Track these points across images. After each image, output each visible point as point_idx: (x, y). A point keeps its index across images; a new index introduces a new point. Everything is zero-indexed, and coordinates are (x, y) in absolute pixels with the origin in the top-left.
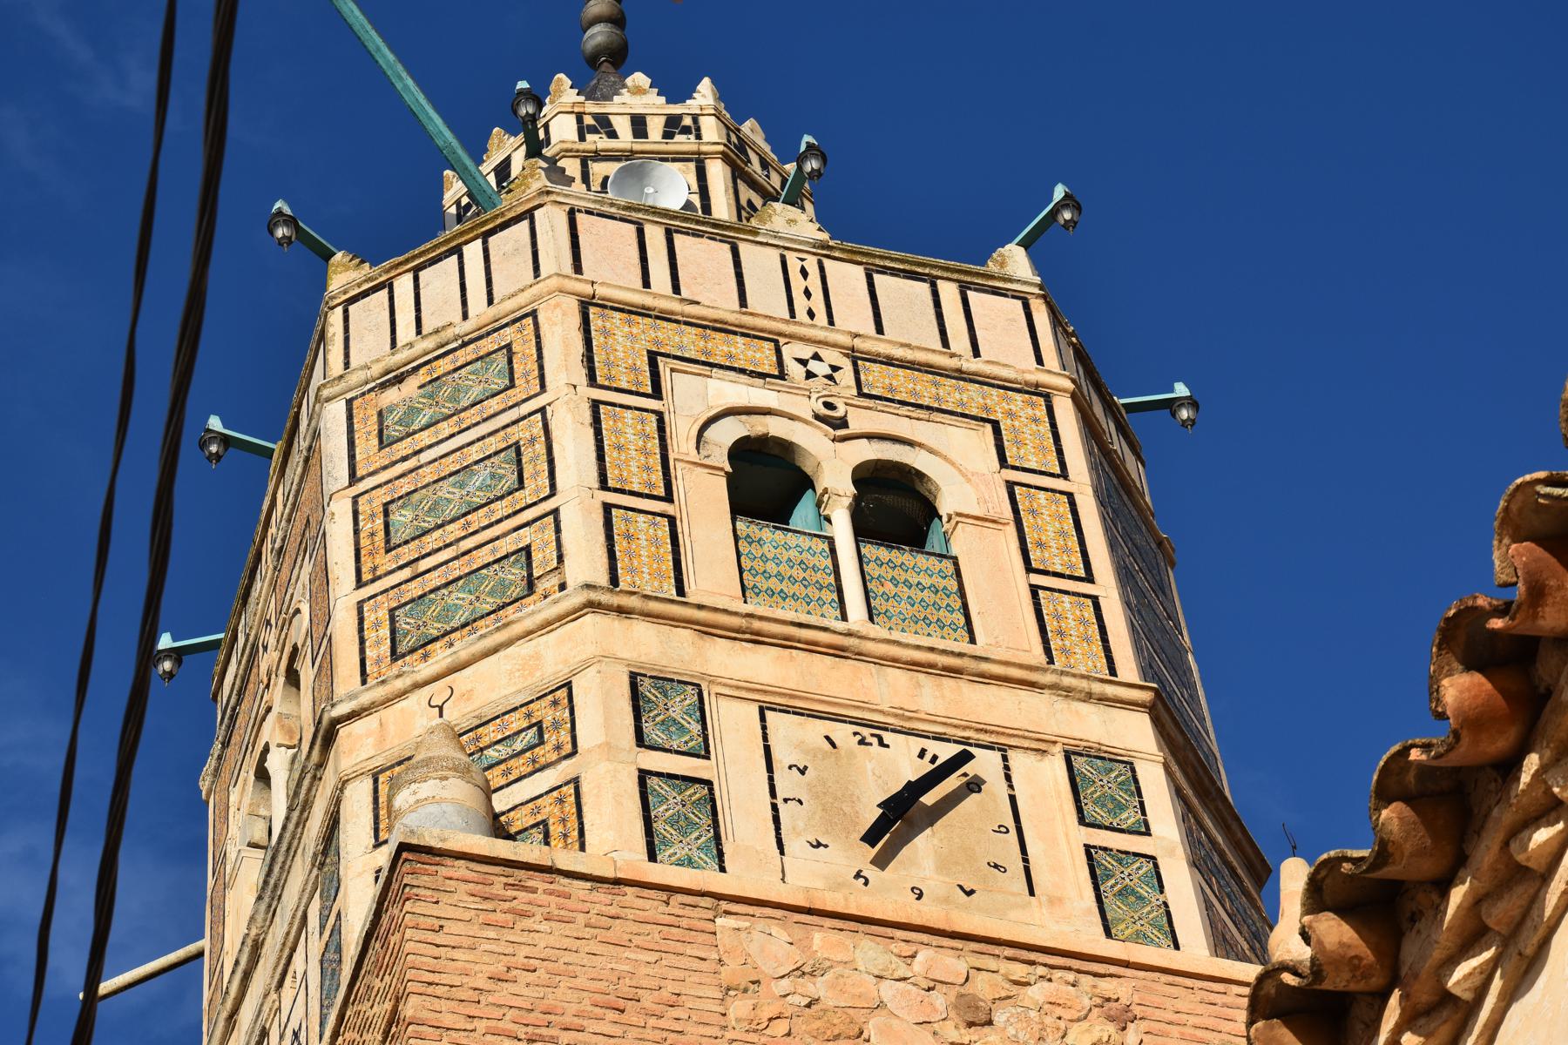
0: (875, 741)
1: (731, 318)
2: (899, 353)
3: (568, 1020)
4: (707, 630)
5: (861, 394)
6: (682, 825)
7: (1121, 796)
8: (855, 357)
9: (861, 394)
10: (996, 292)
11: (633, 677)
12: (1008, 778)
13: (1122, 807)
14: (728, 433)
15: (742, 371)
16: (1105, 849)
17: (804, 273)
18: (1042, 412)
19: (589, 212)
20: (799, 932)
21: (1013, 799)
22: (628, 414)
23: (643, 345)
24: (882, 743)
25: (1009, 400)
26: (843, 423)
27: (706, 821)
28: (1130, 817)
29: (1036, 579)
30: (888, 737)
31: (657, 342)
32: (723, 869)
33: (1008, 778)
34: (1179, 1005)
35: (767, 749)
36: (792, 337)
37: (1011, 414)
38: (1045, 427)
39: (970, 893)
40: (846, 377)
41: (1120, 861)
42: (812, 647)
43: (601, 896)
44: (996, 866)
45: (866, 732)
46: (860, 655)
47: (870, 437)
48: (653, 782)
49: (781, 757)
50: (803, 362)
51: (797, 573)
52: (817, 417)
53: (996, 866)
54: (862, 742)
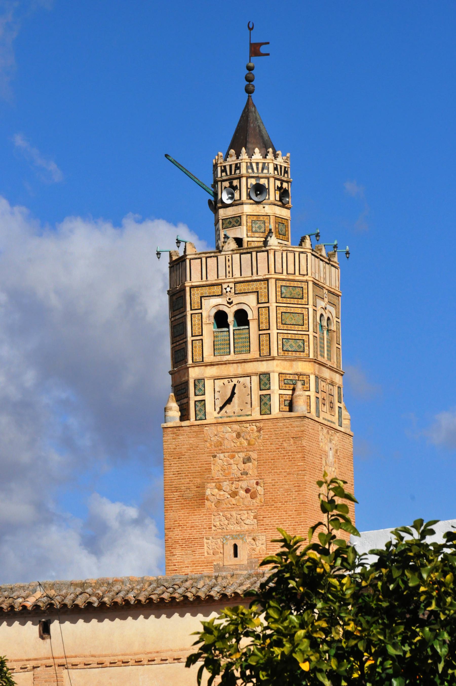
0: (230, 381)
1: (214, 282)
2: (242, 279)
3: (184, 454)
4: (206, 366)
5: (235, 294)
6: (200, 410)
7: (267, 382)
8: (235, 283)
9: (235, 294)
10: (263, 251)
11: (195, 380)
12: (251, 382)
13: (267, 384)
14: (214, 311)
15: (215, 296)
16: (263, 395)
17: (229, 260)
18: (266, 286)
19: (193, 259)
20: (216, 427)
21: (251, 387)
22: (196, 315)
23: (200, 295)
24: (232, 382)
25: (261, 284)
26: (232, 302)
27: (204, 408)
28: (268, 386)
29: (261, 332)
30: (233, 379)
31: (202, 294)
32: (206, 419)
33: (251, 382)
34: (269, 425)
35: (214, 389)
36: (224, 283)
37: (261, 288)
38: (266, 290)
39: (242, 410)
40: (233, 291)
41: (265, 397)
42: (221, 364)
43: (188, 428)
44: (246, 403)
45: (229, 379)
46: (229, 363)
47: (236, 304)
48: (197, 403)
49: (217, 390)
50: (226, 289)
51: (223, 342)
52: (228, 303)
53: (246, 403)
54: (229, 382)
